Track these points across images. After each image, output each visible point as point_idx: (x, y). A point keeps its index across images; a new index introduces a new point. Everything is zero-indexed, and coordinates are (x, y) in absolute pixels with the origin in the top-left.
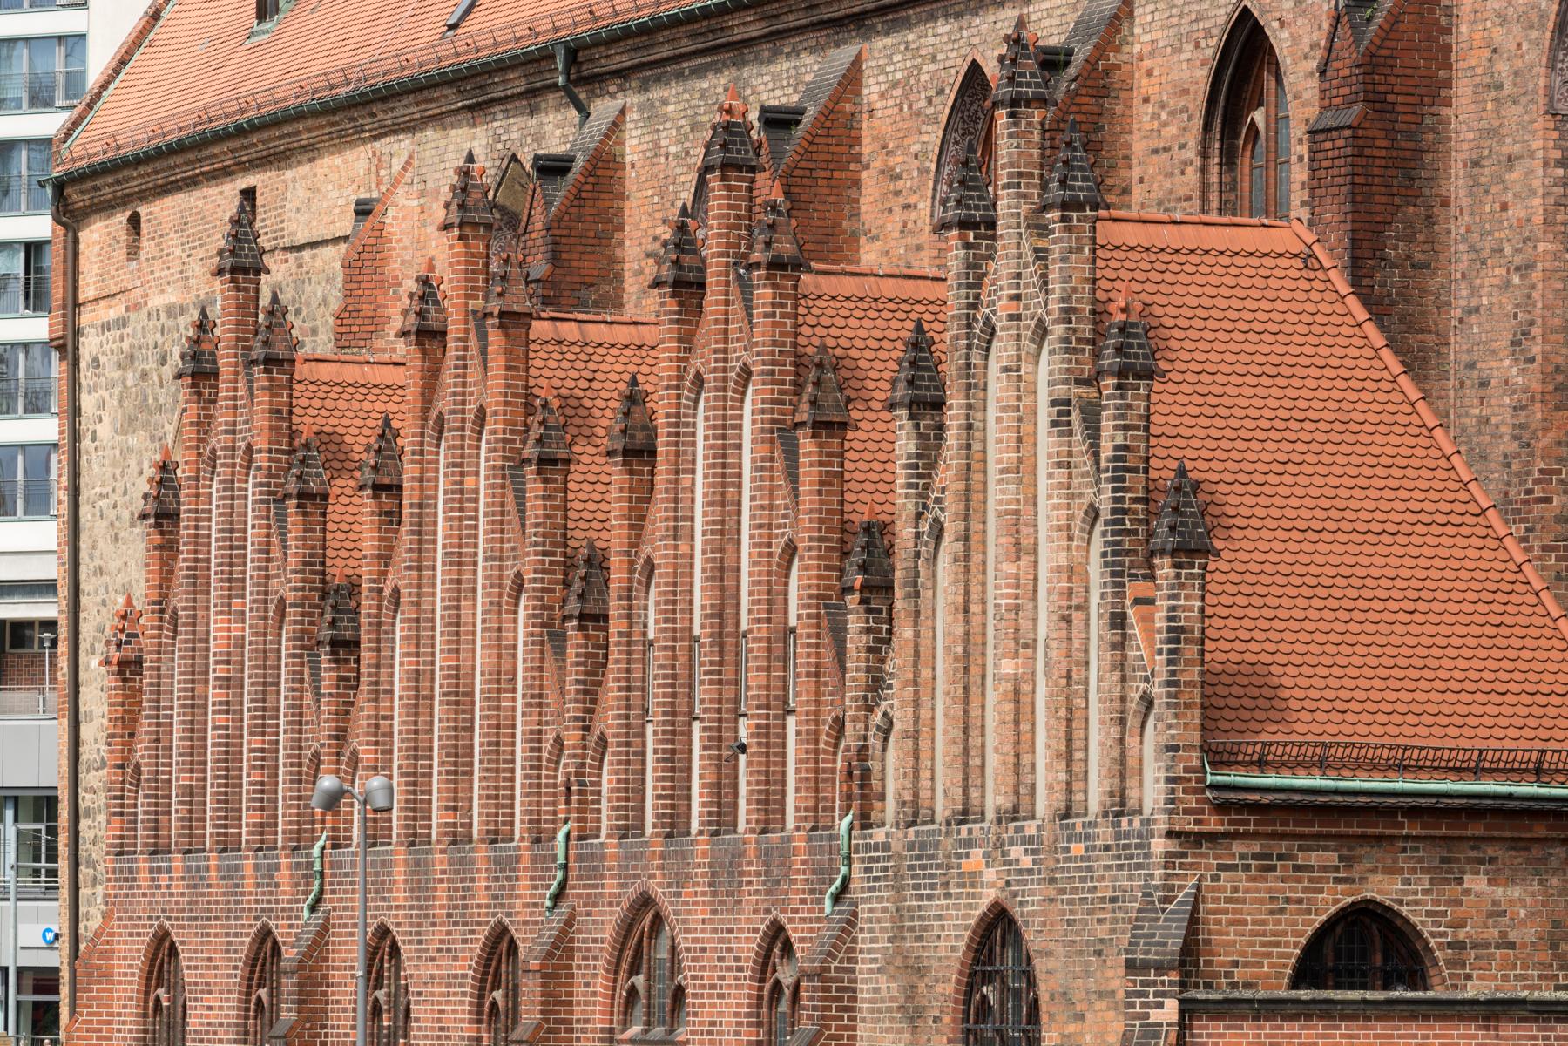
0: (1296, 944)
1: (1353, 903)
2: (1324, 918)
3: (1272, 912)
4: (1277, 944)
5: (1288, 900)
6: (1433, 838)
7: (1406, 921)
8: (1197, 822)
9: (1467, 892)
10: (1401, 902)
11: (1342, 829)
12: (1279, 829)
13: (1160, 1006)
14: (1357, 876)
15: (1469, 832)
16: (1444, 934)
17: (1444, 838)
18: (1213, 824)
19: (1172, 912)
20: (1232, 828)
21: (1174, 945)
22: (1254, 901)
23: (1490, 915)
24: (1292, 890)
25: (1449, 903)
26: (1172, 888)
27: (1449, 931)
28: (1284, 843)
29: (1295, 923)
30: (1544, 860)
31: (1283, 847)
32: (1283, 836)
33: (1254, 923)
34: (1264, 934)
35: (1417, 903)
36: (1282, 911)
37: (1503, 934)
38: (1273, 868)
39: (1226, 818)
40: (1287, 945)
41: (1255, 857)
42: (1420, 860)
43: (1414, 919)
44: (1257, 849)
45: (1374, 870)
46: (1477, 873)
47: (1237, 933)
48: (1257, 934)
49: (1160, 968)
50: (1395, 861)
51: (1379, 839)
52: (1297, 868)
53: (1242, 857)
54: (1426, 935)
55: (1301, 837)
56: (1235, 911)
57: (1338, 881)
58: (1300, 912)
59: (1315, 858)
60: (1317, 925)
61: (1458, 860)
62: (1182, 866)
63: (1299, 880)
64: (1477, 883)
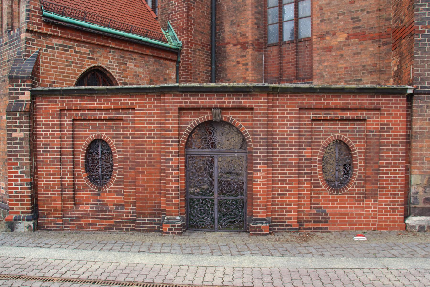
0: (75, 78)
1: (94, 67)
2: (85, 70)
3: (67, 66)
4: (69, 77)
5: (72, 62)
6: (119, 49)
7: (111, 74)
8: (38, 28)
9: (128, 68)
10: (109, 68)
11: (91, 41)
12: (70, 37)
13: (23, 94)
14: (95, 58)
15: (129, 49)
16: (121, 80)
17: (122, 50)
18: (45, 30)
19: (28, 60)
20: (52, 33)
21: (29, 71)
22: (60, 61)
23: (134, 75)
24: (74, 59)
25: (123, 70)
26: (28, 52)
27: (123, 79)
28: (71, 43)
29: (75, 70)
30: (148, 61)
31: (71, 44)
32: (71, 40)
33: (61, 68)
34: (64, 73)
35: (114, 69)
36: (70, 66)
37: (138, 82)
38: (67, 51)
39: (50, 29)
40: (72, 77)
41: (61, 45)
42: (115, 56)
43: (113, 74)
44: (62, 43)
45: (101, 57)
46: (131, 62)
47: (54, 71)
48: (62, 72)
49: (23, 79)
50: (107, 55)
51: (103, 46)
52: (76, 52)
53: (56, 45)
54: (116, 79)
55: (77, 41)
56: (53, 63)
57: (89, 58)
58: (76, 67)
59: (82, 50)
60: (82, 72)
61: (125, 58)
62: (32, 44)
63: (77, 56)
64: (131, 65)
